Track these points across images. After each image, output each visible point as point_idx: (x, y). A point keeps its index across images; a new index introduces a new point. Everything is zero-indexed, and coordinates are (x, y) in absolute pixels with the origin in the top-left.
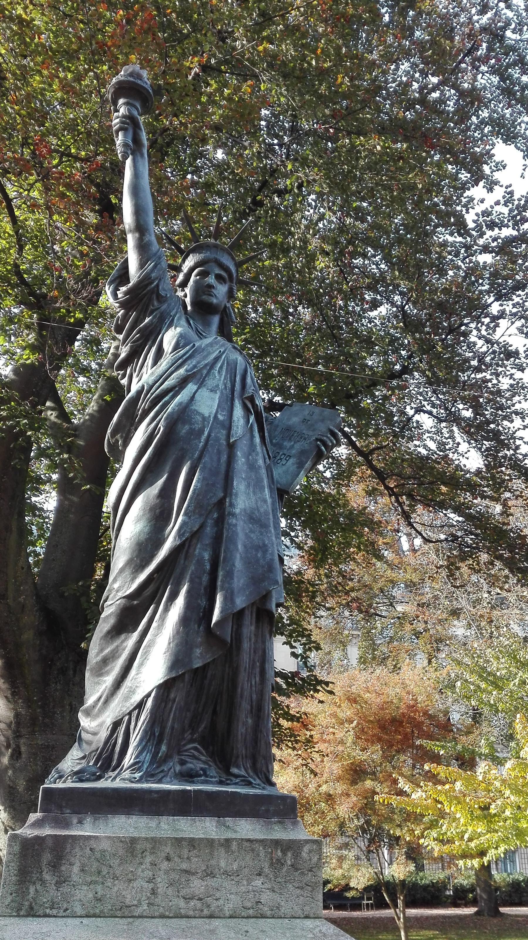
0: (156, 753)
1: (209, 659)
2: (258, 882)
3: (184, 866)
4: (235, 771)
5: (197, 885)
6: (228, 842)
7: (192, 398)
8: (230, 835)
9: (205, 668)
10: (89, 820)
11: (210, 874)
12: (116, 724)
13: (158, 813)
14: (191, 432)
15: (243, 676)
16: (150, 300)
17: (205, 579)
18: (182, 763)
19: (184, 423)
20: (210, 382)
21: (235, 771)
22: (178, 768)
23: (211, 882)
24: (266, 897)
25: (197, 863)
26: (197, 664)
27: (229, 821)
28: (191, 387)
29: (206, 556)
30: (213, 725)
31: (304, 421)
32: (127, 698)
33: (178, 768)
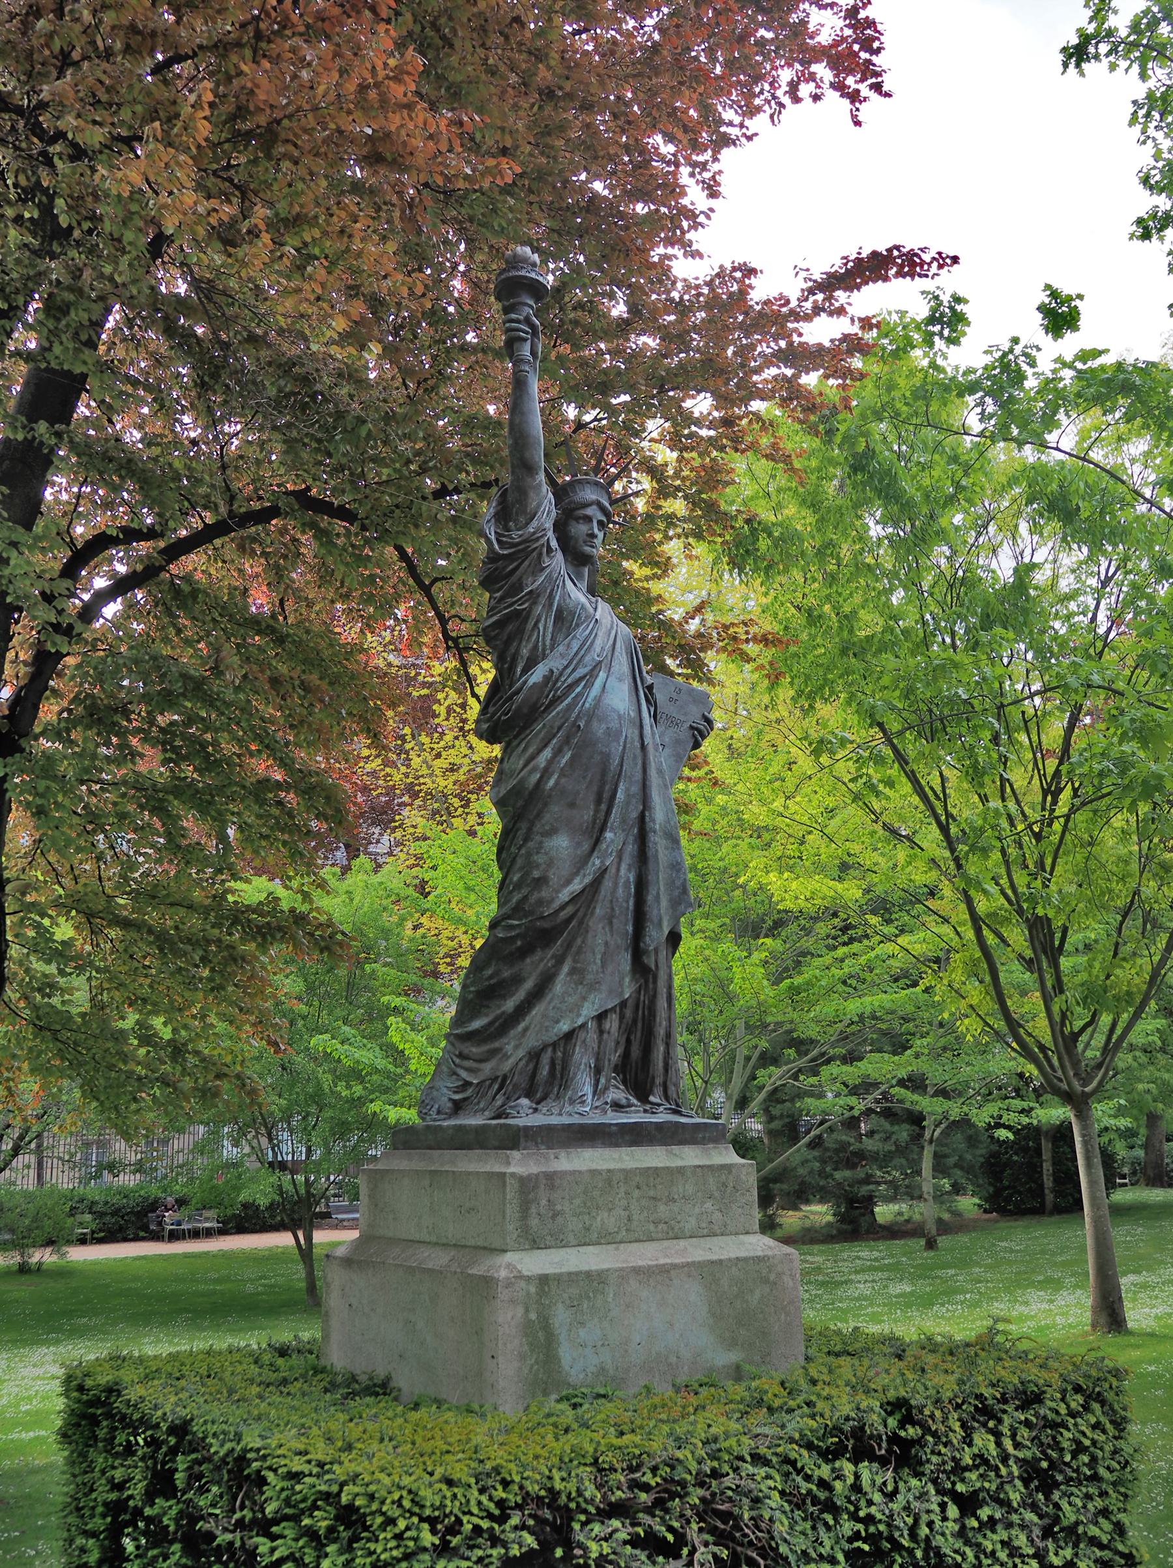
3: (652, 1193)
4: (652, 1098)
10: (563, 1154)
12: (535, 1056)
13: (617, 1145)
16: (540, 554)
20: (615, 667)
21: (652, 1098)
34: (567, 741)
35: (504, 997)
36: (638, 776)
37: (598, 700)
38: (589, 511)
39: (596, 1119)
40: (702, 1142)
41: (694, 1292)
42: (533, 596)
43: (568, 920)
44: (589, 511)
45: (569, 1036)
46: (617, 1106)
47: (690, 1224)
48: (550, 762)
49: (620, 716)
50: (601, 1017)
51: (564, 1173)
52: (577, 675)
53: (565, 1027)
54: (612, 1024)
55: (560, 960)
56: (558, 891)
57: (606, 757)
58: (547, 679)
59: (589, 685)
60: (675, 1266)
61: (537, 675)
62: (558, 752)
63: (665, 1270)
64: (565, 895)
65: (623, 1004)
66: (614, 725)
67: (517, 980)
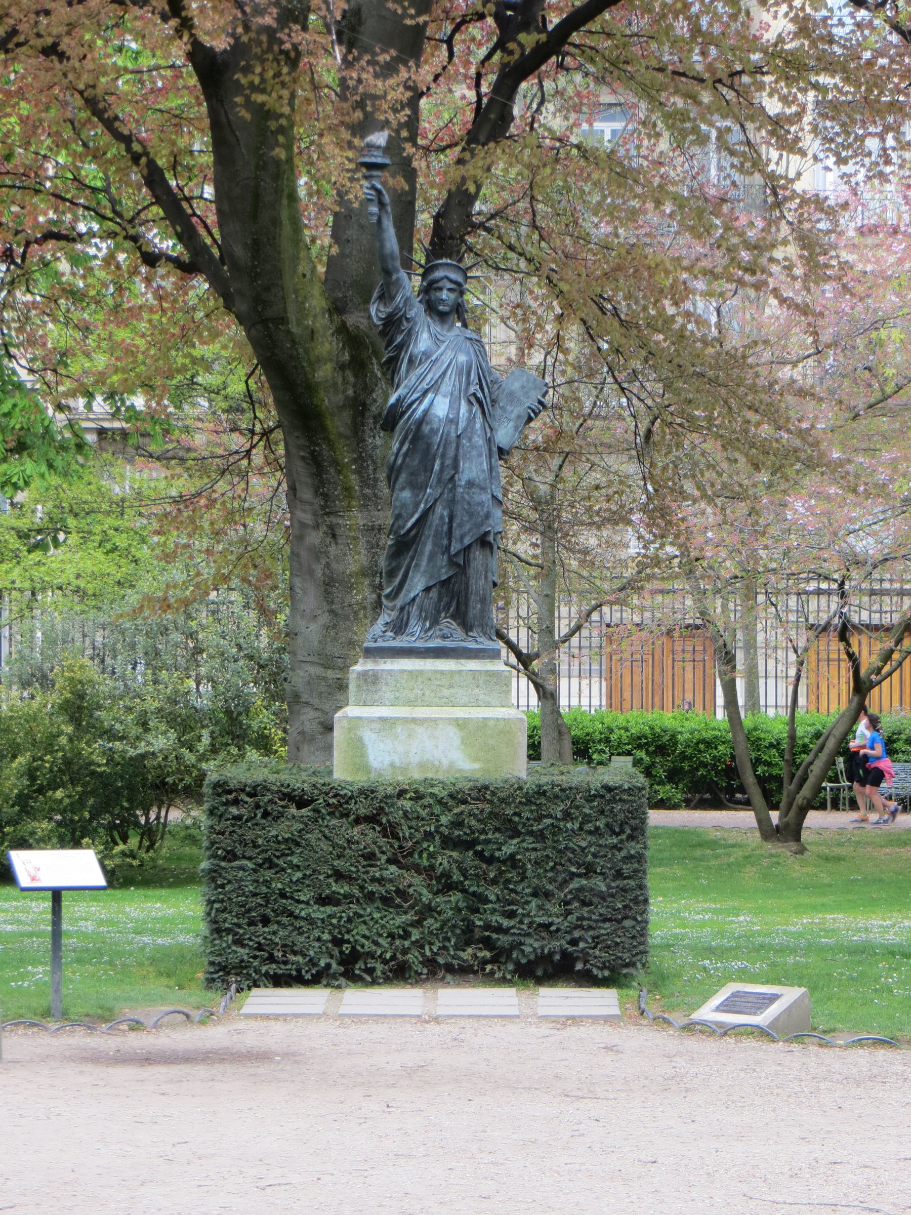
0: (424, 625)
1: (451, 573)
2: (477, 691)
5: (446, 692)
6: (460, 671)
7: (432, 403)
8: (463, 668)
9: (449, 578)
10: (389, 660)
11: (451, 686)
12: (402, 609)
14: (432, 430)
15: (472, 581)
17: (445, 528)
18: (441, 630)
19: (427, 424)
22: (438, 633)
23: (452, 690)
24: (482, 697)
25: (445, 682)
26: (444, 577)
27: (463, 661)
28: (430, 396)
29: (446, 513)
30: (458, 607)
31: (523, 387)
32: (406, 595)
33: (438, 633)
34: (405, 438)
35: (395, 576)
36: (451, 453)
37: (426, 412)
38: (440, 284)
39: (419, 644)
40: (483, 658)
41: (453, 735)
42: (402, 346)
43: (416, 536)
44: (440, 284)
45: (414, 599)
46: (444, 637)
47: (465, 700)
48: (399, 450)
49: (440, 420)
50: (427, 590)
51: (383, 671)
52: (413, 398)
53: (412, 595)
54: (434, 594)
55: (412, 559)
56: (407, 521)
57: (429, 445)
58: (398, 400)
59: (420, 403)
60: (441, 719)
61: (392, 400)
62: (402, 444)
63: (435, 720)
64: (409, 524)
65: (444, 583)
66: (435, 426)
67: (398, 568)
